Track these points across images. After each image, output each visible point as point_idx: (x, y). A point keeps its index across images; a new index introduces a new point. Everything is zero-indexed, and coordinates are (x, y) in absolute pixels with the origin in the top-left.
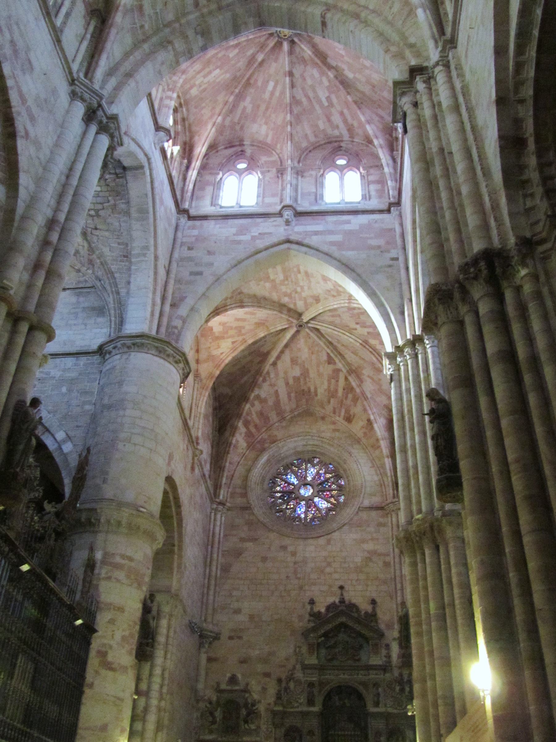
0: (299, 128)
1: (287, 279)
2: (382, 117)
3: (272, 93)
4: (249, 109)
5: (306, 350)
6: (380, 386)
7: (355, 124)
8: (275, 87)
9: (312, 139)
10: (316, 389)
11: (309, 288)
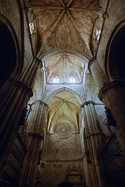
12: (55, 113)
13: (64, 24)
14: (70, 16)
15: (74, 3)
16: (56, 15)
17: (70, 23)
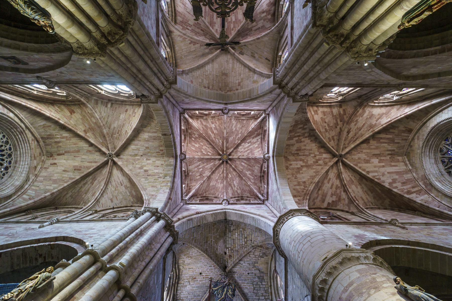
0: (255, 154)
1: (303, 160)
2: (252, 122)
3: (245, 163)
4: (249, 172)
5: (360, 155)
6: (383, 114)
7: (256, 133)
8: (243, 162)
9: (260, 149)
10: (388, 150)
11: (311, 150)
12: (63, 127)
13: (318, 153)
14: (331, 164)
15: (347, 170)
16: (331, 138)
17: (321, 165)
